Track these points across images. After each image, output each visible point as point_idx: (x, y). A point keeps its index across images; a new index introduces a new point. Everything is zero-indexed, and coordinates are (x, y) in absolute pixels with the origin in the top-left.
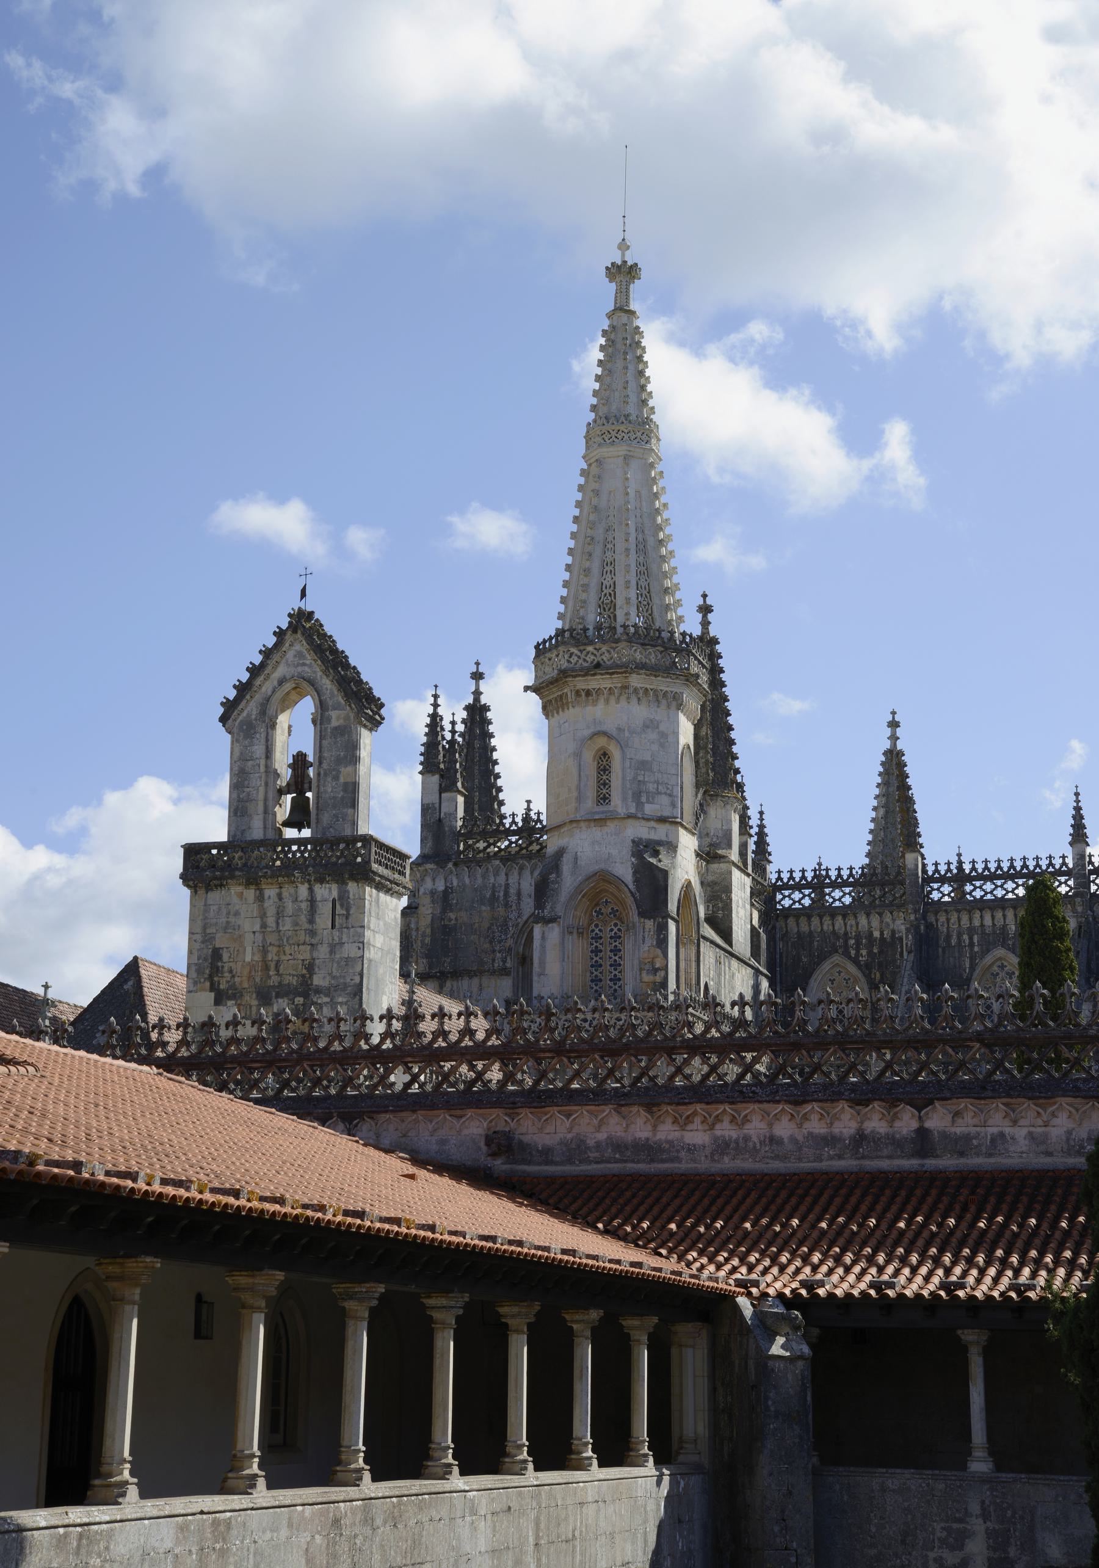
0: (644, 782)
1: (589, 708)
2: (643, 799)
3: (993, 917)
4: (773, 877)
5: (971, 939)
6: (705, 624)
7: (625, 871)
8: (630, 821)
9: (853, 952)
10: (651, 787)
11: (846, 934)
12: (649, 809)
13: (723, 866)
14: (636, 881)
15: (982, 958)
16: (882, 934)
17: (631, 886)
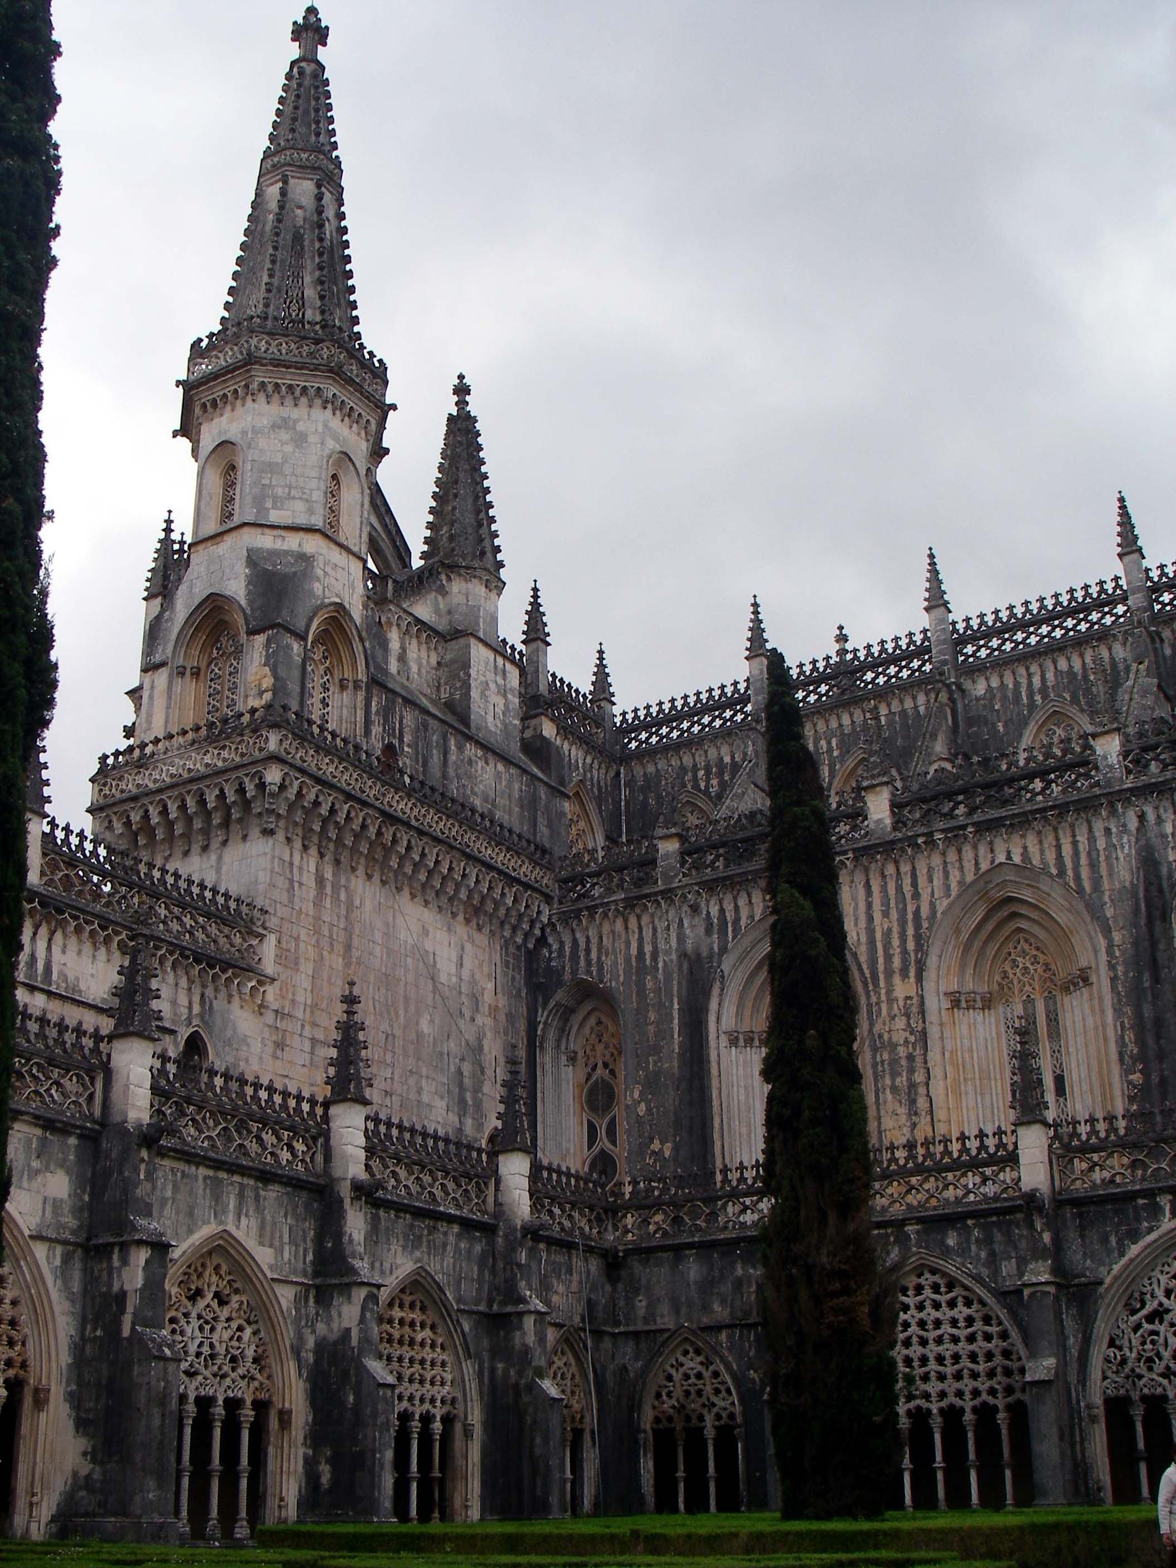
0: (270, 486)
1: (216, 420)
2: (269, 505)
3: (851, 715)
4: (618, 720)
5: (829, 743)
6: (462, 404)
7: (237, 588)
8: (246, 530)
9: (702, 785)
10: (279, 491)
11: (695, 765)
12: (275, 517)
13: (462, 641)
14: (249, 593)
15: (842, 762)
16: (733, 757)
17: (243, 603)
